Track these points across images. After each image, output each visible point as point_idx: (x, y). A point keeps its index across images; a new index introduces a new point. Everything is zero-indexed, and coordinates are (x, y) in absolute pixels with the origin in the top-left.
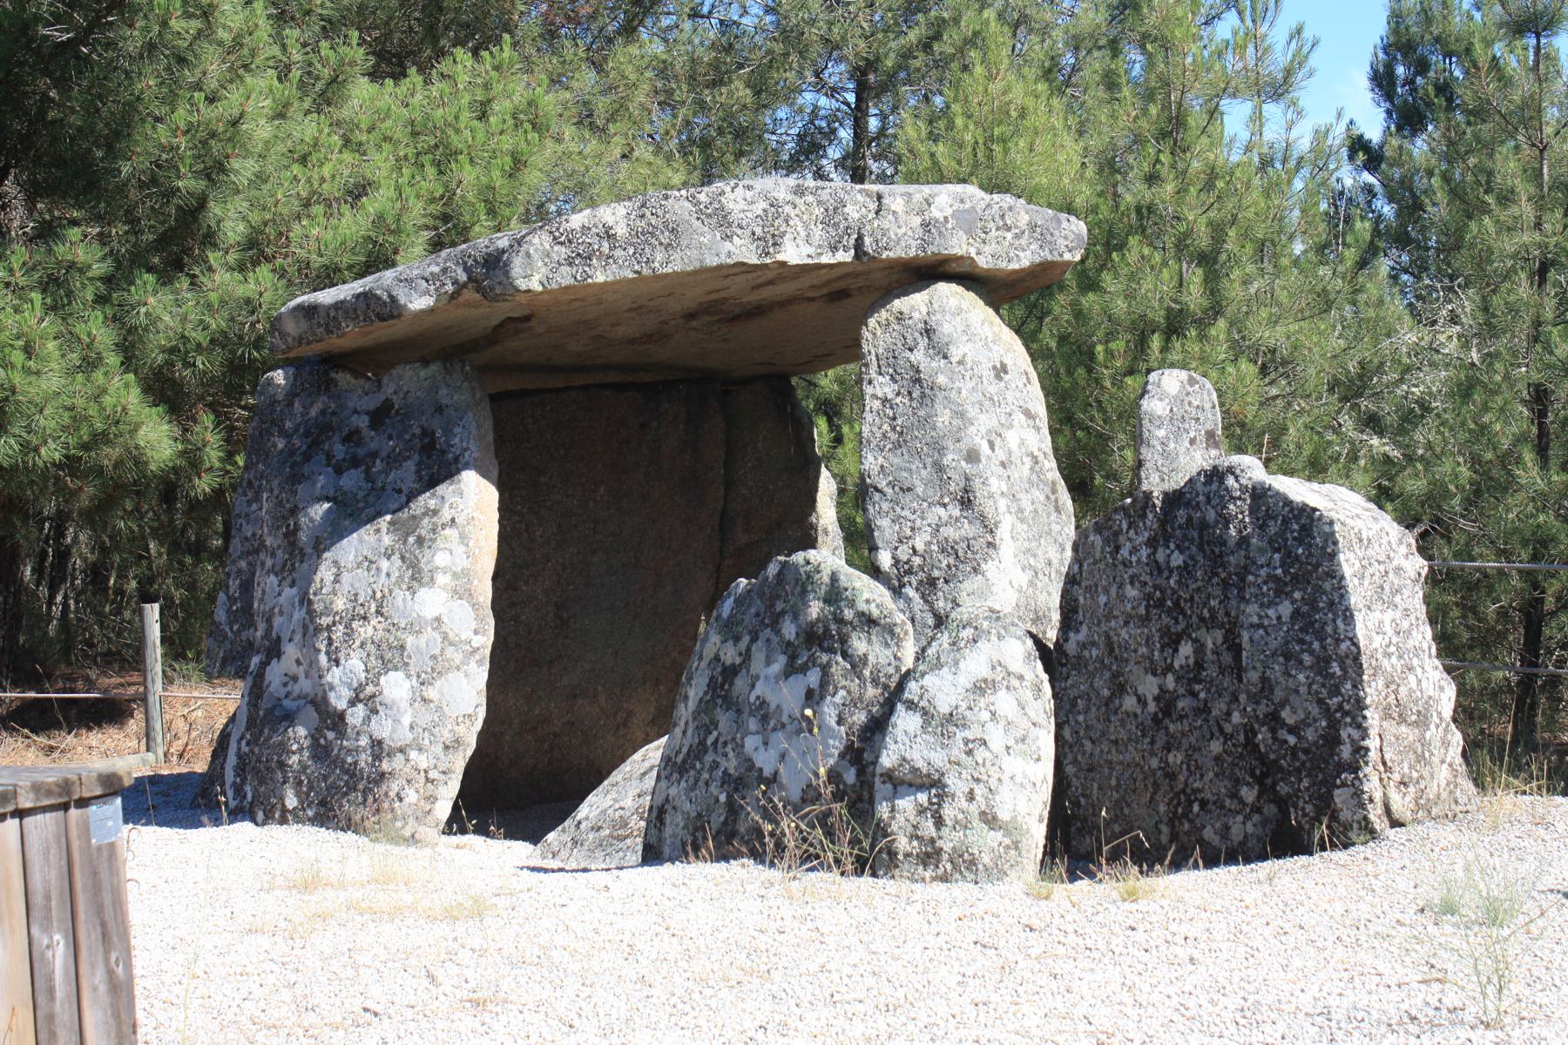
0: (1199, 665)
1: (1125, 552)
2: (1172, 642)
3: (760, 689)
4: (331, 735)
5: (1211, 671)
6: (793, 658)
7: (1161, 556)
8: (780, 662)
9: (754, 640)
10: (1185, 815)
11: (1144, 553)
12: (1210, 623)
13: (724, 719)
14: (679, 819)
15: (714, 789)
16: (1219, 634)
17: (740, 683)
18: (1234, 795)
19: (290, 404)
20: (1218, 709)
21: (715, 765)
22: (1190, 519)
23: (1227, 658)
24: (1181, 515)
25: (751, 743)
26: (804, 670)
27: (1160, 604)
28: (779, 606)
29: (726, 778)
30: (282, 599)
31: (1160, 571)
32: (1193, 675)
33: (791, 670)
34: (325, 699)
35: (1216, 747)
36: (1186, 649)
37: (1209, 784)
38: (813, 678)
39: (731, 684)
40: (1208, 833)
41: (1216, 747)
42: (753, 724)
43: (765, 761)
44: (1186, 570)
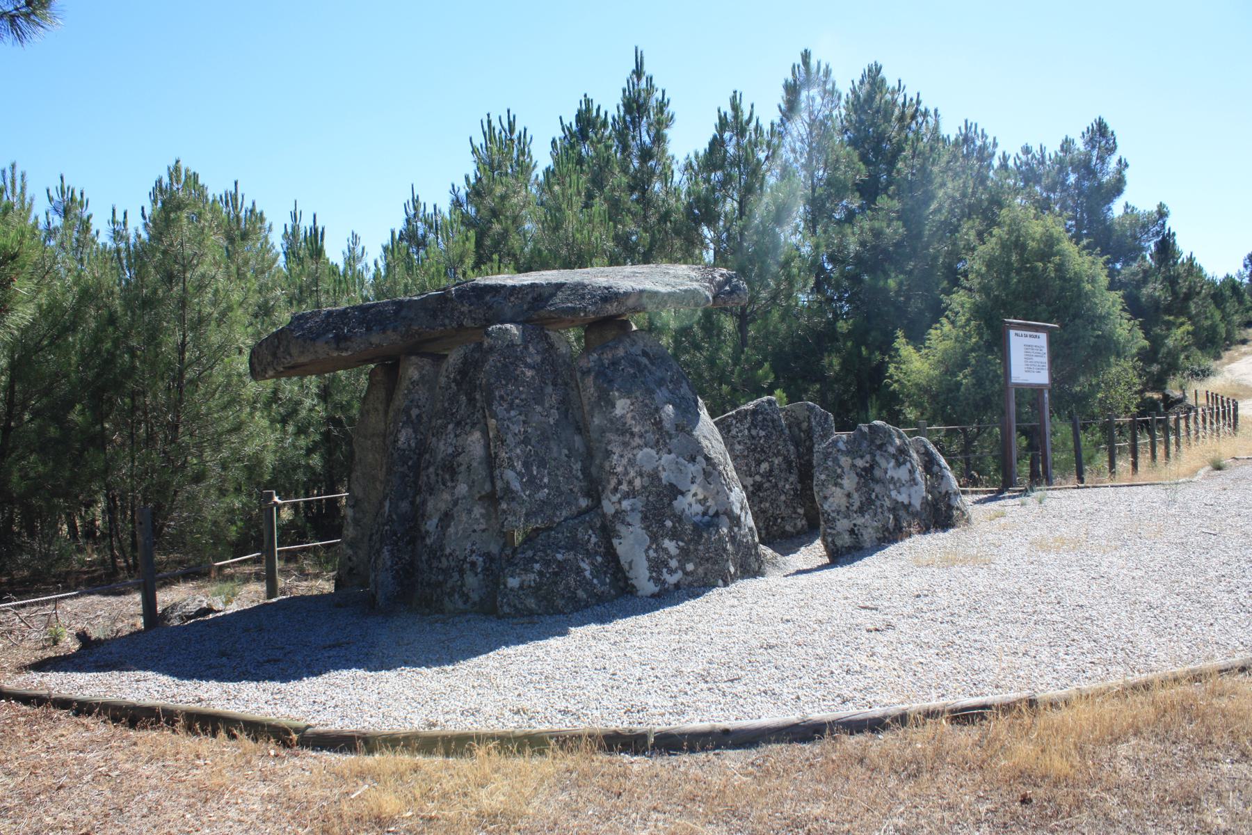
0: (771, 470)
1: (734, 432)
2: (759, 463)
3: (889, 473)
4: (736, 529)
5: (777, 472)
6: (897, 460)
7: (754, 432)
8: (892, 463)
9: (874, 456)
10: (774, 524)
11: (746, 432)
12: (777, 455)
13: (878, 488)
14: (870, 530)
15: (886, 514)
16: (781, 458)
17: (878, 473)
18: (796, 512)
19: (526, 348)
20: (781, 484)
21: (882, 506)
22: (764, 419)
23: (784, 466)
24: (760, 417)
25: (894, 493)
26: (904, 463)
27: (754, 450)
28: (878, 442)
29: (889, 510)
30: (662, 462)
31: (753, 438)
32: (770, 472)
33: (899, 464)
34: (732, 511)
35: (783, 498)
36: (765, 466)
37: (786, 512)
38: (908, 465)
39: (872, 474)
40: (788, 528)
41: (783, 498)
42: (891, 487)
43: (903, 498)
44: (766, 437)
